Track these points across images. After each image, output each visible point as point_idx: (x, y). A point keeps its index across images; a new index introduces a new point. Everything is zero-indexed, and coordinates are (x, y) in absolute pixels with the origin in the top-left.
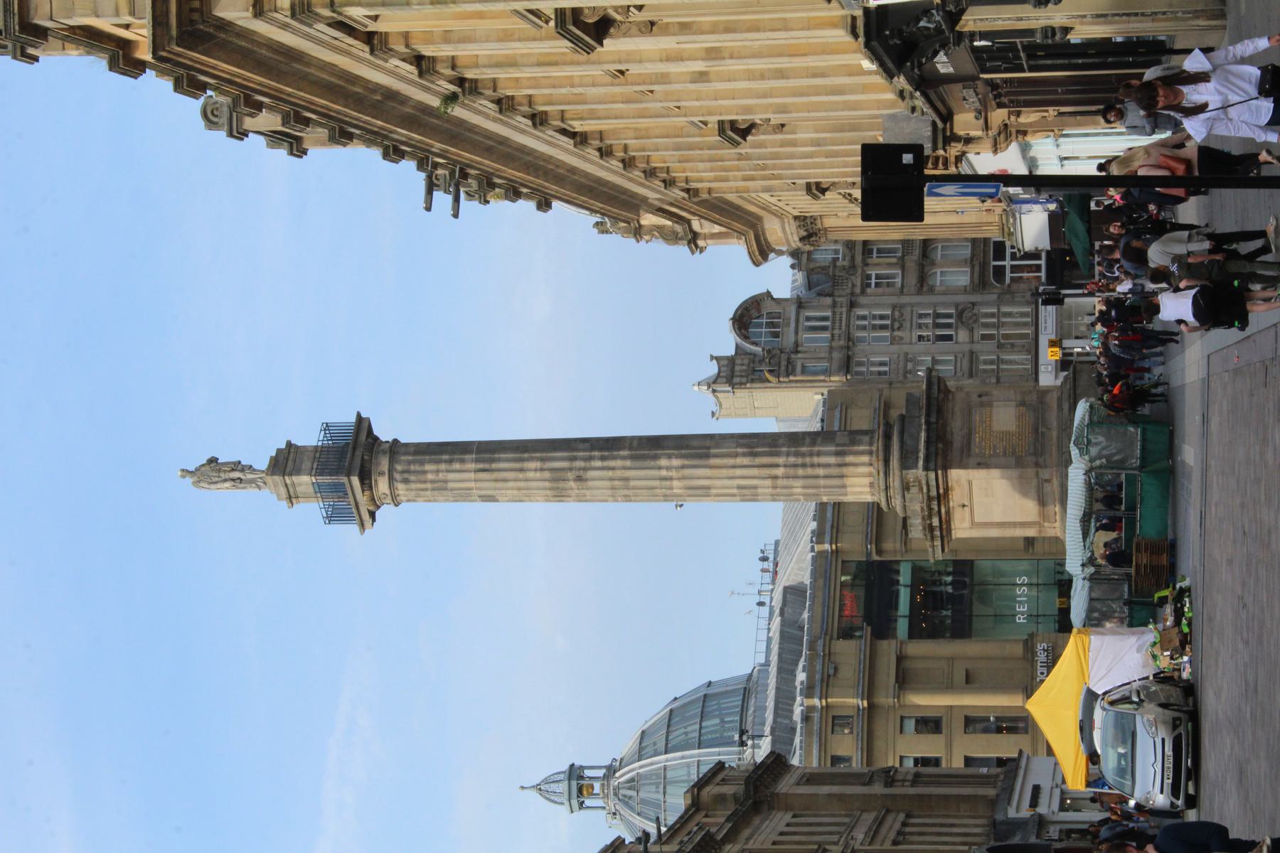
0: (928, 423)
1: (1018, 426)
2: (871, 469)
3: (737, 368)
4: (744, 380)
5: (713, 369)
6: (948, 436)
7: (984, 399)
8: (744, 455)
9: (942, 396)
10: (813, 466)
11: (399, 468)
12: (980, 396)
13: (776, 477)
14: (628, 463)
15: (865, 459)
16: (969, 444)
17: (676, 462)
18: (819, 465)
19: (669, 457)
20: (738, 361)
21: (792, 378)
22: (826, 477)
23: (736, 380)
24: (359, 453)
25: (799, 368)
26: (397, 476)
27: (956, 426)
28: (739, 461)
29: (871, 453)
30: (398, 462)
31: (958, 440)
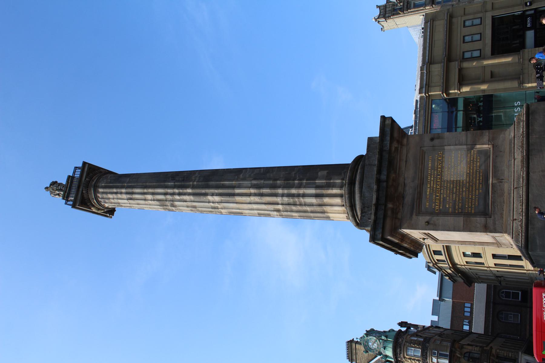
0: (379, 182)
1: (468, 175)
2: (343, 208)
3: (387, 9)
4: (390, 15)
5: (377, 12)
6: (400, 189)
7: (436, 142)
8: (255, 195)
9: (395, 145)
10: (301, 205)
11: (100, 195)
12: (432, 139)
13: (278, 211)
14: (192, 198)
15: (338, 201)
16: (420, 198)
17: (217, 198)
18: (305, 205)
19: (213, 195)
20: (388, 6)
21: (409, 11)
22: (312, 212)
23: (387, 15)
24: (81, 190)
25: (412, 6)
26: (100, 200)
27: (408, 174)
28: (253, 199)
29: (341, 196)
30: (99, 192)
31: (408, 199)
